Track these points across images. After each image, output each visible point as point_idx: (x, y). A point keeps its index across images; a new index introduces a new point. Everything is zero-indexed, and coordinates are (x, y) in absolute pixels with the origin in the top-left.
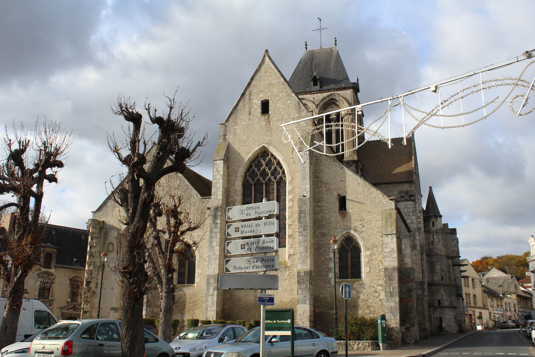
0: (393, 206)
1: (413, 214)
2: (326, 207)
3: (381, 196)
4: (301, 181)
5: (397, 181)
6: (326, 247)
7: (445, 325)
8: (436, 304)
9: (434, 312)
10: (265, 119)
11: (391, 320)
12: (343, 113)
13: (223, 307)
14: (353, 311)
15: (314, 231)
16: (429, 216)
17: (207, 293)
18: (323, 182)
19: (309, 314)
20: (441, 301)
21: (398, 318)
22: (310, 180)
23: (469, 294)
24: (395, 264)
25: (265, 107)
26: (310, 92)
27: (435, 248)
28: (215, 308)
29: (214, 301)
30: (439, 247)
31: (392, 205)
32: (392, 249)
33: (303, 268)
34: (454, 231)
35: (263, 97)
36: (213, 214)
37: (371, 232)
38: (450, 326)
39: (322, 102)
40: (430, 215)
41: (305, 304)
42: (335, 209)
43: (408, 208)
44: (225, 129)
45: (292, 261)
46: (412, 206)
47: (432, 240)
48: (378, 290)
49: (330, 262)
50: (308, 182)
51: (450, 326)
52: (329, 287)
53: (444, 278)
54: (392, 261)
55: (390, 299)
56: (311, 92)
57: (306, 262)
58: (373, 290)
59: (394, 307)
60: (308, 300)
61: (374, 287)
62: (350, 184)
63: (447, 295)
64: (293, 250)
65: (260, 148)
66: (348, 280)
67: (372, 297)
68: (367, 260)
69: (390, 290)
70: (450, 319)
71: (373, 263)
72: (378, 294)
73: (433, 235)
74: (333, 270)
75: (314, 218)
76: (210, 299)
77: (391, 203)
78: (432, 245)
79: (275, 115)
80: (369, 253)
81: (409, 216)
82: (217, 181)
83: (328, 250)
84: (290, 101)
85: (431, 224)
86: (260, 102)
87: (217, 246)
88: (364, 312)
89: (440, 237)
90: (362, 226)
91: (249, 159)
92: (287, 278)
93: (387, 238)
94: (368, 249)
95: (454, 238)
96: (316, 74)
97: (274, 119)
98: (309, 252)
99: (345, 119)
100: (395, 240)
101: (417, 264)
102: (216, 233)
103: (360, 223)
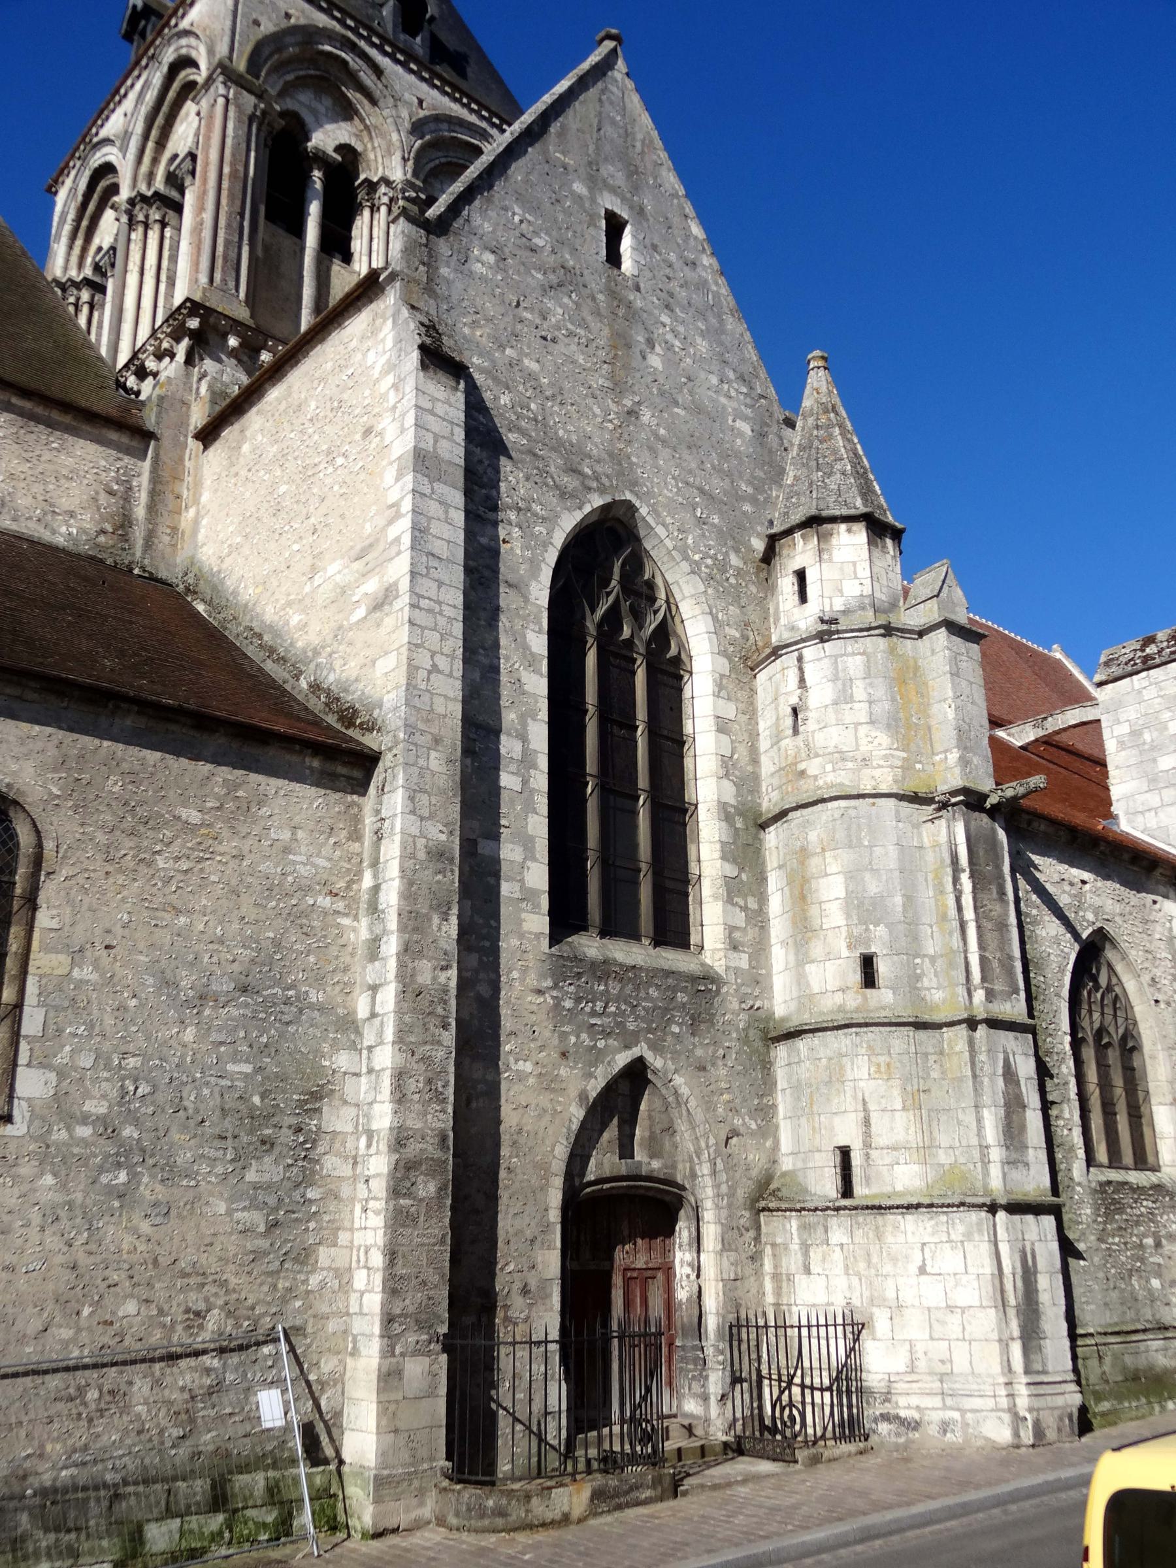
7: (898, 1363)
8: (827, 1185)
9: (806, 1248)
20: (856, 1160)
27: (811, 753)
47: (794, 700)
53: (883, 968)
70: (951, 1308)
78: (796, 731)
89: (854, 665)
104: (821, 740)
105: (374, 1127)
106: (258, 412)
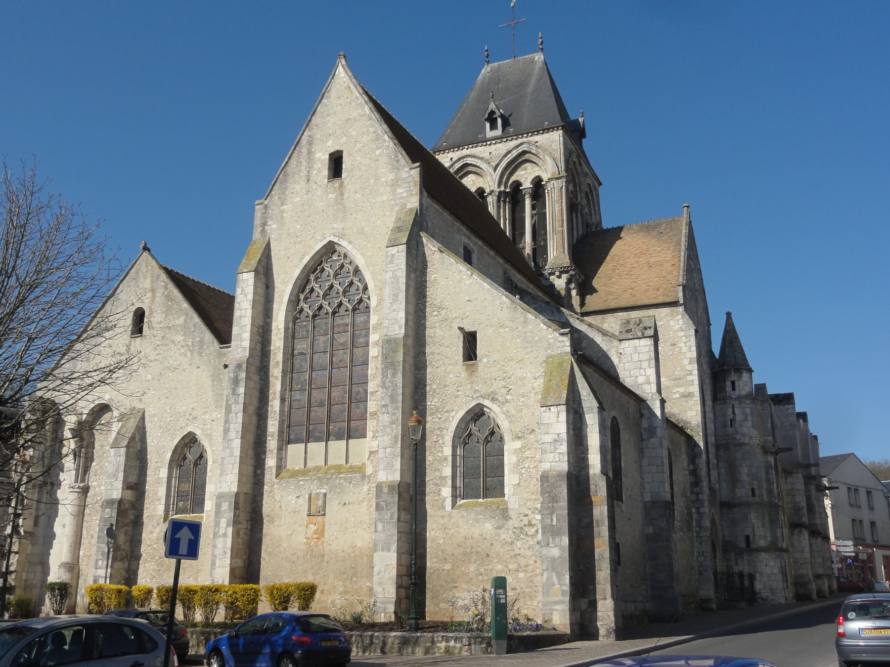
0: (566, 348)
1: (649, 365)
2: (438, 354)
3: (545, 327)
4: (389, 305)
5: (646, 302)
6: (438, 435)
8: (743, 545)
10: (335, 188)
11: (554, 585)
12: (545, 177)
13: (249, 557)
14: (486, 565)
15: (416, 402)
16: (724, 370)
17: (216, 530)
18: (435, 305)
19: (396, 573)
20: (751, 538)
21: (567, 581)
22: (406, 302)
23: (861, 521)
24: (564, 466)
25: (336, 163)
26: (484, 141)
27: (737, 432)
28: (228, 561)
29: (227, 548)
30: (745, 430)
31: (565, 346)
32: (558, 436)
33: (387, 479)
34: (787, 399)
35: (332, 146)
36: (233, 377)
37: (523, 402)
38: (771, 589)
39: (506, 159)
40: (725, 368)
41: (389, 551)
42: (457, 358)
43: (639, 354)
44: (264, 214)
45: (374, 464)
46: (647, 349)
48: (534, 522)
49: (445, 465)
50: (403, 306)
51: (771, 589)
52: (441, 516)
53: (757, 492)
54: (558, 460)
55: (551, 540)
56: (486, 141)
57: (393, 466)
58: (526, 522)
59: (560, 558)
60: (394, 543)
61: (526, 515)
62: (486, 306)
63: (763, 526)
64: (376, 442)
65: (324, 246)
66: (481, 500)
67: (523, 537)
68: (514, 459)
69: (552, 521)
70: (772, 574)
71: (527, 466)
72: (535, 529)
73: (733, 407)
74: (450, 482)
75: (416, 378)
76: (220, 542)
77: (563, 341)
79: (353, 179)
80: (518, 444)
81: (641, 369)
82: (243, 311)
83: (441, 441)
84: (381, 150)
85: (729, 384)
86: (328, 156)
87: (236, 438)
88: (506, 567)
89: (748, 410)
90: (504, 391)
91: (304, 268)
92: (364, 498)
93: (548, 414)
94: (519, 438)
95: (790, 412)
96: (494, 106)
97: (350, 186)
98: (400, 446)
99: (549, 189)
100: (563, 416)
101: (657, 466)
102: (236, 413)
103: (503, 383)
104: (739, 430)
105: (702, 525)
106: (611, 316)
